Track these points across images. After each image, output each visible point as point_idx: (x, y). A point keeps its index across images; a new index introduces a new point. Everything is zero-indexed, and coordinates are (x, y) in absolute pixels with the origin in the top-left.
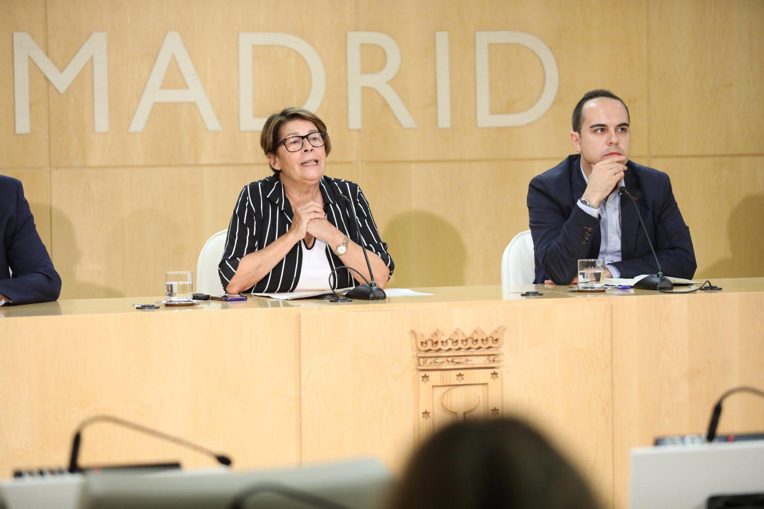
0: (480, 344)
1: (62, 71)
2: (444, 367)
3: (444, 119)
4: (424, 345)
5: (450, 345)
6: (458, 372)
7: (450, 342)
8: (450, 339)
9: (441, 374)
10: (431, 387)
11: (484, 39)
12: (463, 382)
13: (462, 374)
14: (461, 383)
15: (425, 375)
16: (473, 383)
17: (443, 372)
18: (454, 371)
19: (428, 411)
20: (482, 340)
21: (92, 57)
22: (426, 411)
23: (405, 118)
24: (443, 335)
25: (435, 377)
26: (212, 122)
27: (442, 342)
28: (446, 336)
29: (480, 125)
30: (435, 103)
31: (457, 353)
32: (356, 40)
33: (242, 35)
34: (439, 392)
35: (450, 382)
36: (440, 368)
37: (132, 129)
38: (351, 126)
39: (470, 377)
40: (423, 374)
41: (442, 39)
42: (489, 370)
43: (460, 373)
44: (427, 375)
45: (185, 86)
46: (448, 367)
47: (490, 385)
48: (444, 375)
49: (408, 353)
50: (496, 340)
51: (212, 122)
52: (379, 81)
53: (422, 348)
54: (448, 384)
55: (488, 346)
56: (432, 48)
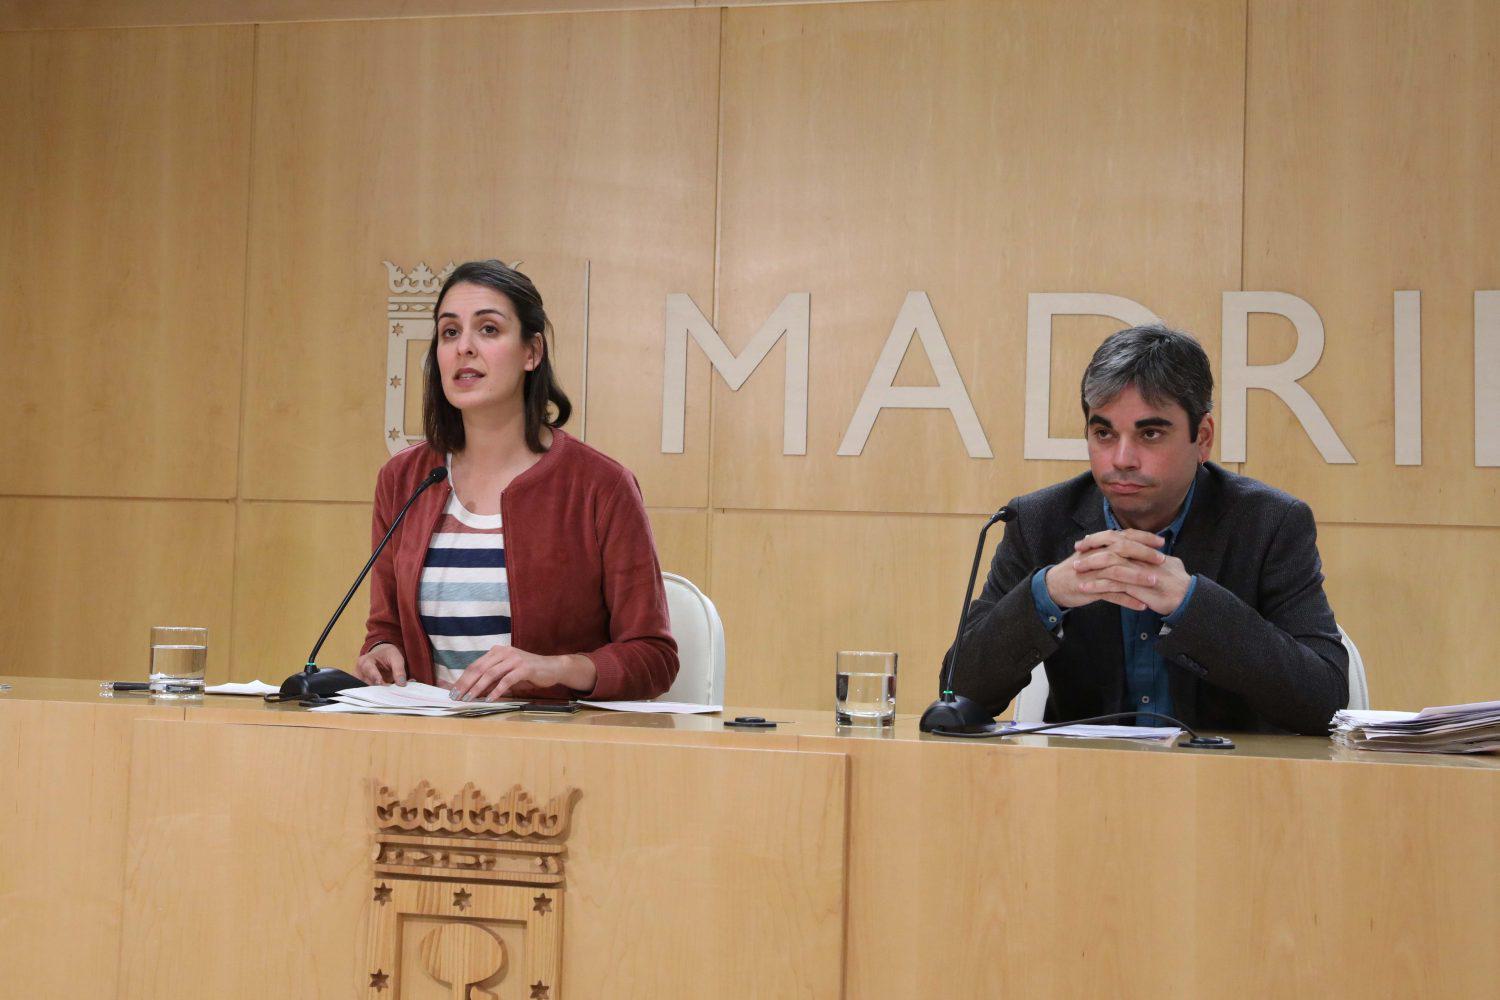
0: (513, 825)
2: (426, 871)
3: (1408, 450)
4: (410, 816)
5: (443, 822)
6: (457, 887)
7: (443, 813)
8: (443, 806)
9: (420, 887)
10: (393, 919)
12: (467, 913)
13: (467, 892)
14: (462, 914)
15: (383, 884)
16: (490, 916)
17: (423, 883)
18: (449, 884)
22: (380, 972)
23: (1332, 448)
24: (431, 793)
25: (405, 894)
27: (428, 814)
28: (436, 798)
30: (1390, 419)
31: (456, 843)
34: (416, 932)
35: (438, 910)
36: (418, 873)
39: (486, 901)
41: (1407, 304)
42: (532, 889)
44: (387, 886)
48: (425, 891)
49: (360, 834)
50: (554, 818)
51: (977, 445)
52: (1280, 379)
54: (434, 912)
55: (531, 832)
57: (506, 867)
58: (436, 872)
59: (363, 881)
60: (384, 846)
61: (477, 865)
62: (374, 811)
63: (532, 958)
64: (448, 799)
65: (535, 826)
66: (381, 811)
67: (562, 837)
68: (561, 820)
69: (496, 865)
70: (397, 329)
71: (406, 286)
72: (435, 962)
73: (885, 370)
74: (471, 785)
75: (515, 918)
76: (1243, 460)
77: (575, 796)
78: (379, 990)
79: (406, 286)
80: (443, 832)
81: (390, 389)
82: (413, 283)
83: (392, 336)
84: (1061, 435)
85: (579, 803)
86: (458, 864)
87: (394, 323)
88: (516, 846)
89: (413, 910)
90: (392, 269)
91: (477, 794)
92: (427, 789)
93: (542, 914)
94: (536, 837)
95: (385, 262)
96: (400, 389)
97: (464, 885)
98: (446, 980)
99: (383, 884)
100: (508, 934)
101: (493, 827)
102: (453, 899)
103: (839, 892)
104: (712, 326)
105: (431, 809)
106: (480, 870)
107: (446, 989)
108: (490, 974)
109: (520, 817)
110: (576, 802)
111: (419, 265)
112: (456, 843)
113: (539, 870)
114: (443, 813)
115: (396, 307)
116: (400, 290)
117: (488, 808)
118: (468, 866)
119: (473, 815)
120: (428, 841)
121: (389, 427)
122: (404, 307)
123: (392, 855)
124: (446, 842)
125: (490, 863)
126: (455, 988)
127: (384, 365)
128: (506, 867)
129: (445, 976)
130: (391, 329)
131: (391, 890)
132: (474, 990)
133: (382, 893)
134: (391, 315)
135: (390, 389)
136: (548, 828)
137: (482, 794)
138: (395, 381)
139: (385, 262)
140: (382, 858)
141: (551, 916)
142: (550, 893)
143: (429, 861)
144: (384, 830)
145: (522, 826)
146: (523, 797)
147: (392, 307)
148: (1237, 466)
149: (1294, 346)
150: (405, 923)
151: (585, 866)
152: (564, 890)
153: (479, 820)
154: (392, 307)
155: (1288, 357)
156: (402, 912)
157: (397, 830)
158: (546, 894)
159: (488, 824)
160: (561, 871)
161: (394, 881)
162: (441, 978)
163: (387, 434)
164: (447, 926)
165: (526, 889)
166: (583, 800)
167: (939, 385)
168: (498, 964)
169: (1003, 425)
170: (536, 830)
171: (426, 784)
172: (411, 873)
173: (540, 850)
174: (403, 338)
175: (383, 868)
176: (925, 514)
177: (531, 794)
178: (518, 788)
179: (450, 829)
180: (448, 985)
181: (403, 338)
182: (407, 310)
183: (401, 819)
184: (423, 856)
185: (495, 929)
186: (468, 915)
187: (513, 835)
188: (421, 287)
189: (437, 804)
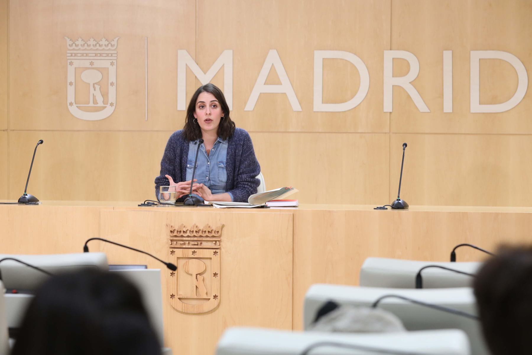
0: (207, 234)
1: (205, 73)
2: (184, 246)
3: (448, 107)
4: (179, 233)
5: (188, 234)
6: (193, 250)
7: (188, 232)
9: (183, 250)
10: (176, 259)
11: (476, 56)
12: (196, 256)
13: (196, 251)
14: (194, 257)
15: (173, 250)
17: (184, 249)
20: (196, 232)
21: (224, 64)
23: (422, 106)
24: (184, 227)
26: (296, 106)
27: (184, 232)
28: (186, 228)
29: (472, 111)
30: (442, 96)
31: (192, 239)
32: (389, 56)
33: (316, 52)
35: (188, 256)
37: (246, 109)
38: (385, 110)
39: (200, 253)
40: (171, 250)
41: (447, 55)
43: (194, 251)
44: (174, 251)
46: (189, 247)
47: (212, 259)
48: (184, 251)
50: (218, 232)
51: (296, 106)
52: (404, 82)
53: (172, 235)
54: (187, 257)
56: (440, 62)
57: (205, 245)
58: (187, 246)
60: (171, 241)
61: (197, 245)
65: (213, 234)
66: (171, 232)
67: (220, 236)
68: (220, 232)
69: (202, 244)
70: (71, 64)
72: (188, 268)
74: (195, 224)
75: (209, 257)
76: (391, 111)
77: (223, 226)
78: (173, 277)
80: (188, 236)
82: (76, 46)
83: (69, 66)
84: (327, 102)
86: (192, 244)
87: (69, 61)
88: (208, 239)
89: (181, 256)
90: (68, 40)
91: (197, 227)
92: (184, 226)
93: (216, 256)
94: (213, 237)
95: (66, 38)
96: (73, 86)
97: (195, 250)
98: (191, 273)
99: (173, 250)
100: (207, 262)
101: (202, 235)
104: (196, 62)
105: (185, 231)
106: (198, 245)
107: (190, 276)
108: (202, 271)
109: (209, 232)
111: (79, 38)
112: (192, 239)
113: (214, 245)
115: (70, 55)
117: (200, 230)
118: (195, 245)
119: (196, 232)
120: (184, 239)
121: (69, 102)
122: (74, 55)
124: (189, 239)
125: (201, 243)
126: (193, 275)
127: (66, 77)
128: (205, 245)
130: (68, 63)
131: (175, 252)
132: (198, 276)
133: (172, 252)
135: (69, 86)
136: (216, 234)
137: (198, 226)
138: (71, 84)
139: (66, 38)
142: (217, 250)
143: (185, 244)
144: (171, 237)
146: (209, 227)
148: (389, 114)
149: (409, 71)
151: (226, 244)
153: (197, 233)
155: (407, 74)
157: (176, 236)
159: (200, 234)
160: (220, 245)
161: (176, 249)
162: (190, 273)
163: (68, 104)
164: (190, 260)
166: (225, 227)
167: (281, 84)
168: (204, 269)
170: (213, 235)
172: (180, 247)
173: (214, 240)
175: (172, 246)
177: (211, 226)
178: (208, 224)
179: (190, 236)
180: (191, 275)
182: (75, 56)
183: (177, 234)
184: (183, 243)
186: (196, 257)
187: (207, 236)
188: (80, 47)
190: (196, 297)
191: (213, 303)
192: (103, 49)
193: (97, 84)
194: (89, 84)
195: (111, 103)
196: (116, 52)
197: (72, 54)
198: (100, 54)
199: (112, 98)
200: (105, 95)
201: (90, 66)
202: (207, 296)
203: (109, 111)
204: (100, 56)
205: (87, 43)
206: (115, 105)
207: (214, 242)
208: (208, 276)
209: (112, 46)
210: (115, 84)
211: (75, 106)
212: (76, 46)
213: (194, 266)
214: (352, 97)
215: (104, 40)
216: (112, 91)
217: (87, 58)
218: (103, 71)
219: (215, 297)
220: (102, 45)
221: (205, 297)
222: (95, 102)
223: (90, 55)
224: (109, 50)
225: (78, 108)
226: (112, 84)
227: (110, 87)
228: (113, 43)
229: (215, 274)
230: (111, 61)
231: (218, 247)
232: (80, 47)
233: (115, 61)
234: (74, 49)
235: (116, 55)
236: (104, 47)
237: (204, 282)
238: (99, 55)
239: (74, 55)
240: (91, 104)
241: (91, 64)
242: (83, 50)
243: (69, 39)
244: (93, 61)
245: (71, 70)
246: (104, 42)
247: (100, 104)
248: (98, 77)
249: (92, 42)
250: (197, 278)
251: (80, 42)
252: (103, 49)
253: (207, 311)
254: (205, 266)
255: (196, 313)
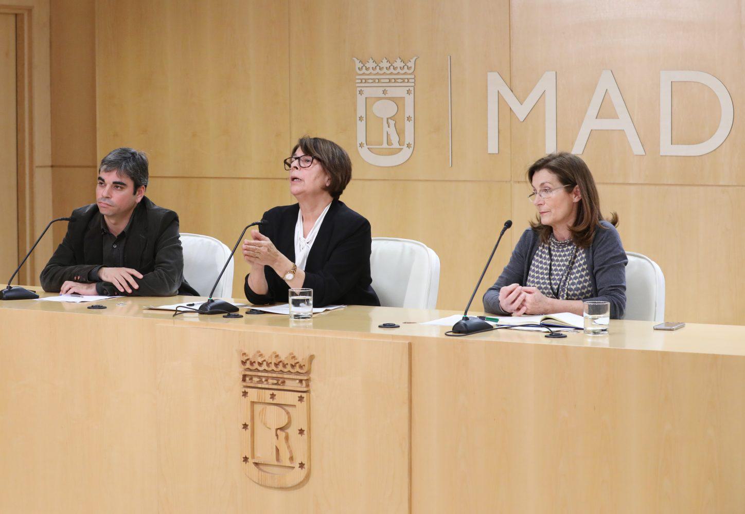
2: (260, 386)
5: (264, 367)
6: (271, 392)
10: (249, 404)
12: (275, 402)
19: (247, 424)
25: (253, 394)
27: (260, 364)
31: (270, 375)
34: (258, 408)
36: (257, 386)
39: (281, 397)
42: (297, 393)
45: (615, 116)
47: (297, 406)
49: (237, 371)
51: (638, 149)
54: (263, 402)
58: (263, 386)
59: (239, 387)
60: (245, 376)
62: (240, 362)
63: (299, 420)
64: (266, 358)
65: (297, 369)
66: (244, 363)
67: (308, 373)
70: (361, 92)
71: (364, 70)
73: (593, 110)
77: (312, 357)
79: (364, 70)
80: (265, 371)
81: (359, 122)
82: (367, 69)
85: (313, 361)
87: (359, 89)
90: (357, 62)
91: (277, 356)
96: (364, 122)
97: (273, 391)
102: (270, 396)
103: (406, 396)
105: (260, 362)
110: (313, 359)
112: (270, 375)
114: (265, 363)
116: (361, 72)
118: (276, 384)
120: (260, 374)
121: (359, 142)
123: (247, 379)
124: (266, 374)
125: (283, 382)
127: (355, 110)
129: (268, 426)
133: (245, 394)
134: (358, 85)
135: (359, 122)
139: (355, 59)
140: (244, 380)
141: (304, 403)
142: (304, 395)
143: (261, 382)
145: (303, 369)
146: (294, 357)
147: (358, 81)
150: (255, 405)
151: (317, 385)
152: (310, 393)
154: (358, 81)
156: (253, 401)
157: (249, 369)
158: (303, 395)
160: (308, 386)
163: (359, 145)
165: (295, 393)
167: (618, 118)
169: (649, 138)
170: (298, 370)
171: (259, 352)
174: (364, 97)
176: (614, 184)
178: (291, 354)
181: (364, 97)
185: (287, 408)
186: (275, 403)
189: (263, 359)
190: (276, 463)
191: (299, 474)
192: (398, 73)
193: (391, 119)
194: (382, 118)
195: (408, 143)
196: (413, 77)
197: (361, 80)
198: (394, 79)
199: (409, 138)
200: (400, 133)
201: (383, 96)
202: (291, 463)
203: (406, 153)
204: (395, 82)
205: (393, 65)
206: (412, 146)
207: (298, 381)
208: (293, 431)
209: (409, 68)
210: (413, 119)
211: (366, 147)
212: (367, 69)
213: (275, 416)
214: (711, 135)
215: (399, 60)
216: (409, 127)
217: (380, 85)
218: (396, 100)
219: (302, 465)
220: (397, 67)
221: (288, 463)
222: (389, 142)
223: (382, 81)
224: (405, 73)
225: (371, 151)
226: (409, 119)
227: (407, 122)
228: (409, 64)
229: (301, 431)
230: (408, 89)
231: (305, 389)
232: (371, 71)
233: (412, 89)
234: (364, 74)
235: (413, 81)
236: (399, 70)
237: (289, 441)
238: (393, 81)
239: (364, 81)
240: (385, 145)
241: (384, 92)
242: (375, 74)
243: (359, 61)
244: (387, 89)
245: (361, 101)
246: (399, 64)
247: (396, 145)
248: (391, 109)
249: (385, 64)
250: (277, 435)
251: (371, 64)
252: (398, 73)
253: (290, 486)
254: (287, 417)
255: (276, 486)
